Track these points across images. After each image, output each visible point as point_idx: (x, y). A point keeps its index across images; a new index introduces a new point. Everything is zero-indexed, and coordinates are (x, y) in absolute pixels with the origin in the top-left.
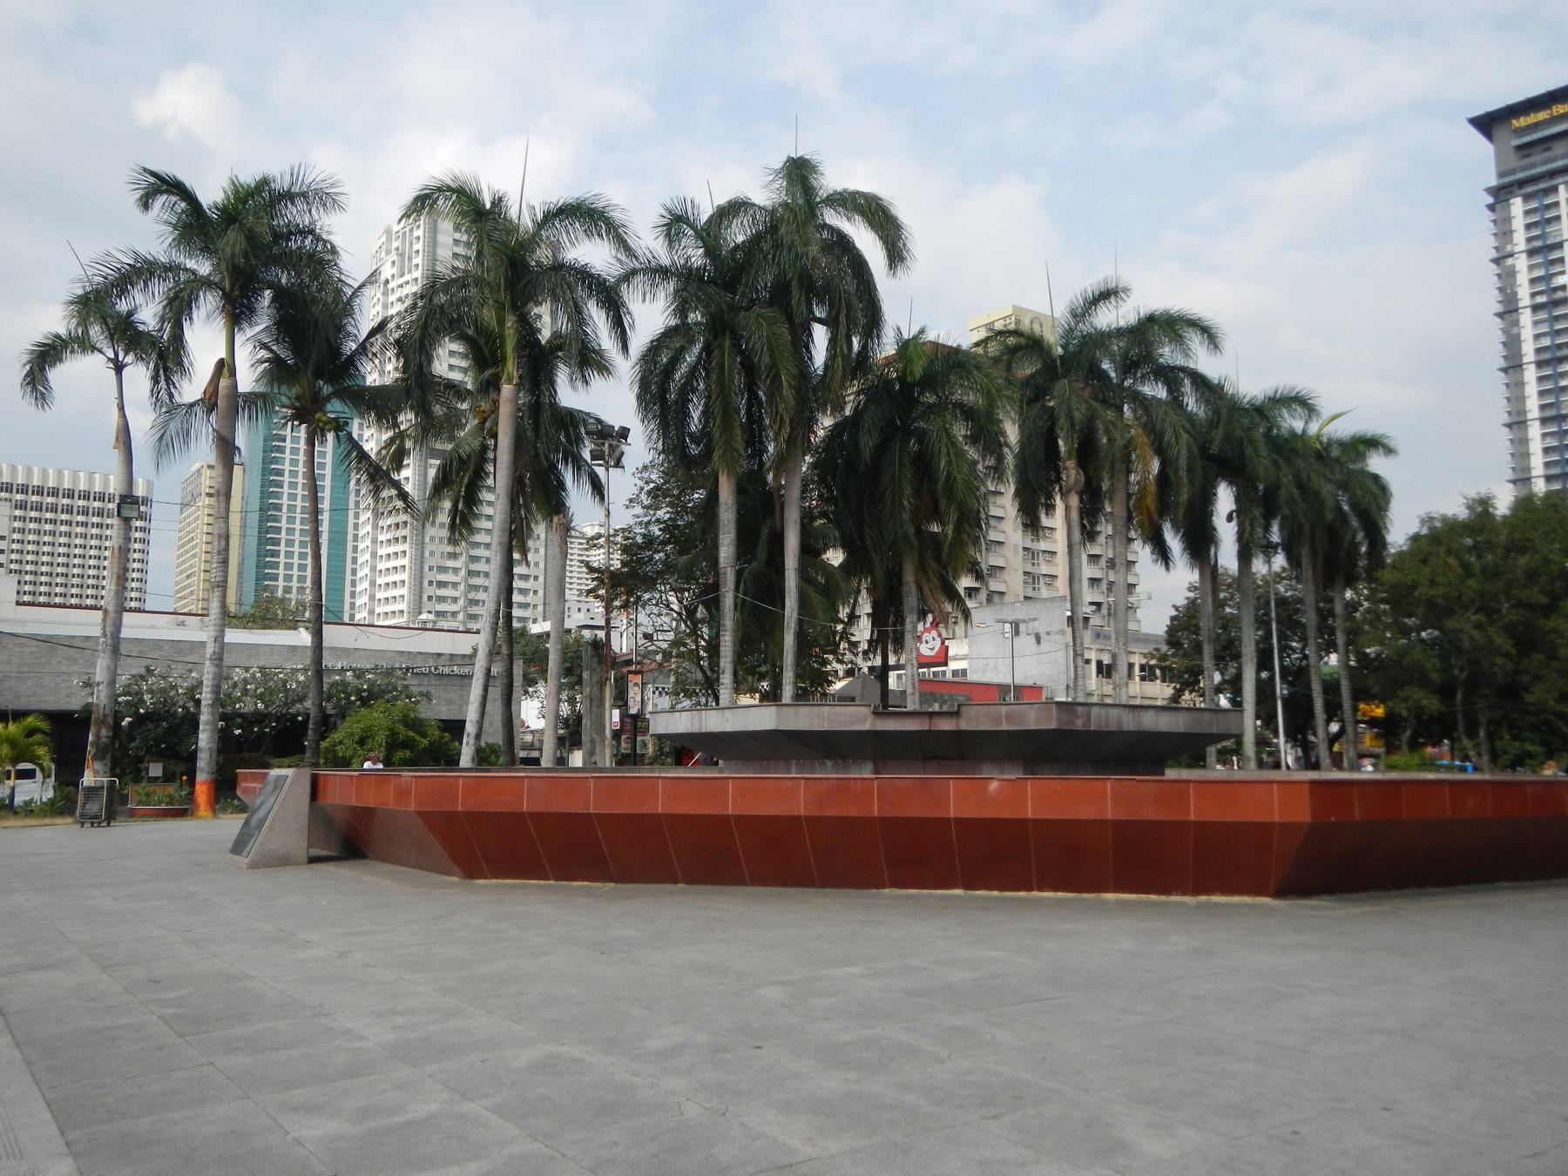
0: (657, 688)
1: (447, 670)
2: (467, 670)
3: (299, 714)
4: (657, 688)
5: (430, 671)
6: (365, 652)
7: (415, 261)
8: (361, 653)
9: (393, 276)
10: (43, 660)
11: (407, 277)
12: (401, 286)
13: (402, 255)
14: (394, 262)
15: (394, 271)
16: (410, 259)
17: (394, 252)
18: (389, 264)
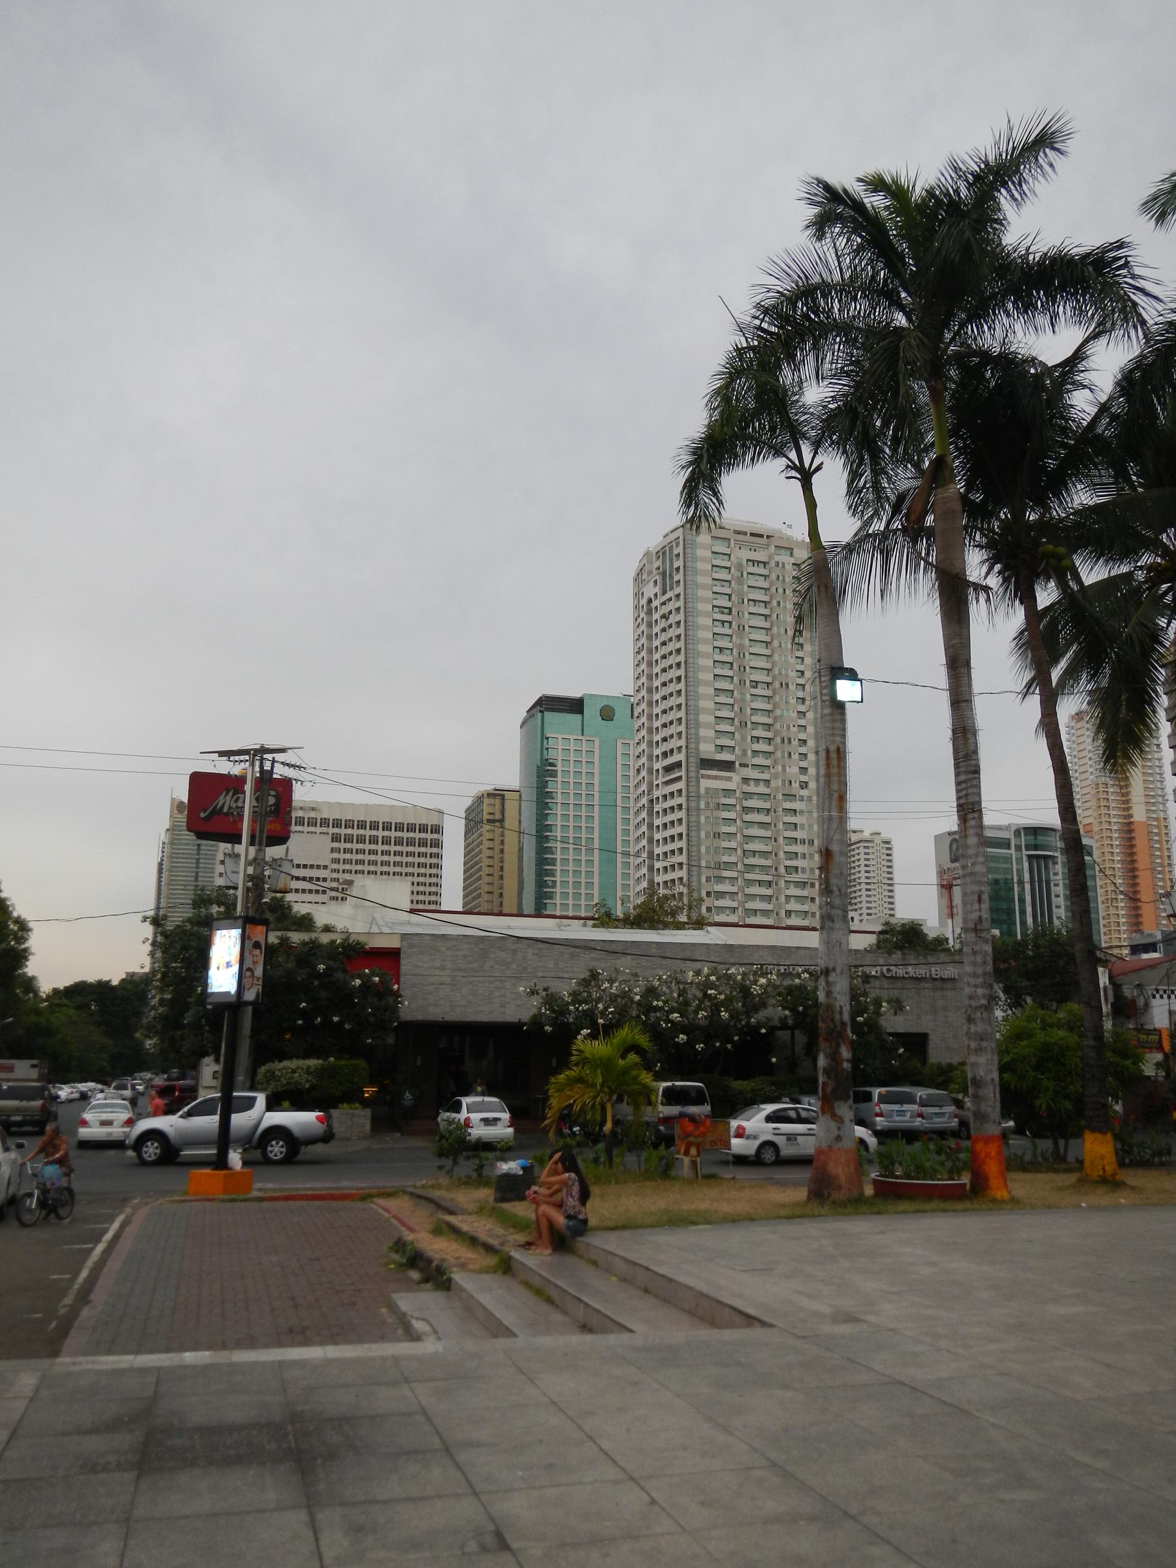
0: (1165, 991)
1: (901, 972)
2: (923, 972)
3: (759, 1025)
4: (1157, 991)
5: (882, 974)
6: (807, 951)
7: (676, 578)
8: (803, 952)
9: (656, 595)
10: (475, 965)
11: (670, 594)
12: (664, 604)
13: (664, 574)
14: (656, 582)
15: (657, 589)
16: (671, 577)
17: (655, 572)
18: (652, 583)
